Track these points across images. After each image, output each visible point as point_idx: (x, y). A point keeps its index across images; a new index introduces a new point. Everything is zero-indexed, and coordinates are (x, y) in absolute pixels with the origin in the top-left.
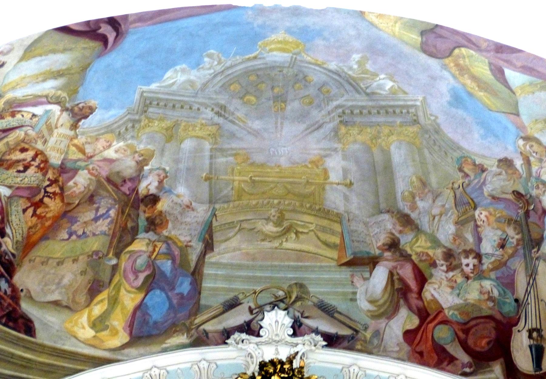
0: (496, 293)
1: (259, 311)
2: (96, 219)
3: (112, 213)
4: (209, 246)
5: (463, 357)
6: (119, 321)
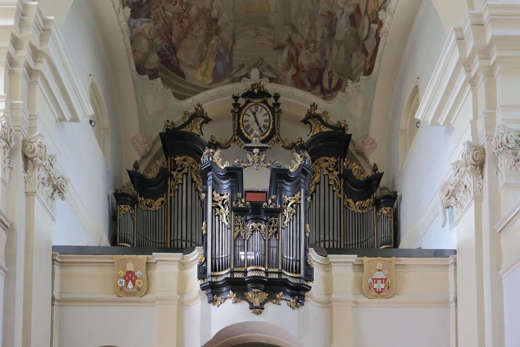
0: (319, 58)
1: (249, 69)
2: (200, 29)
3: (204, 26)
4: (234, 42)
5: (309, 84)
6: (209, 73)
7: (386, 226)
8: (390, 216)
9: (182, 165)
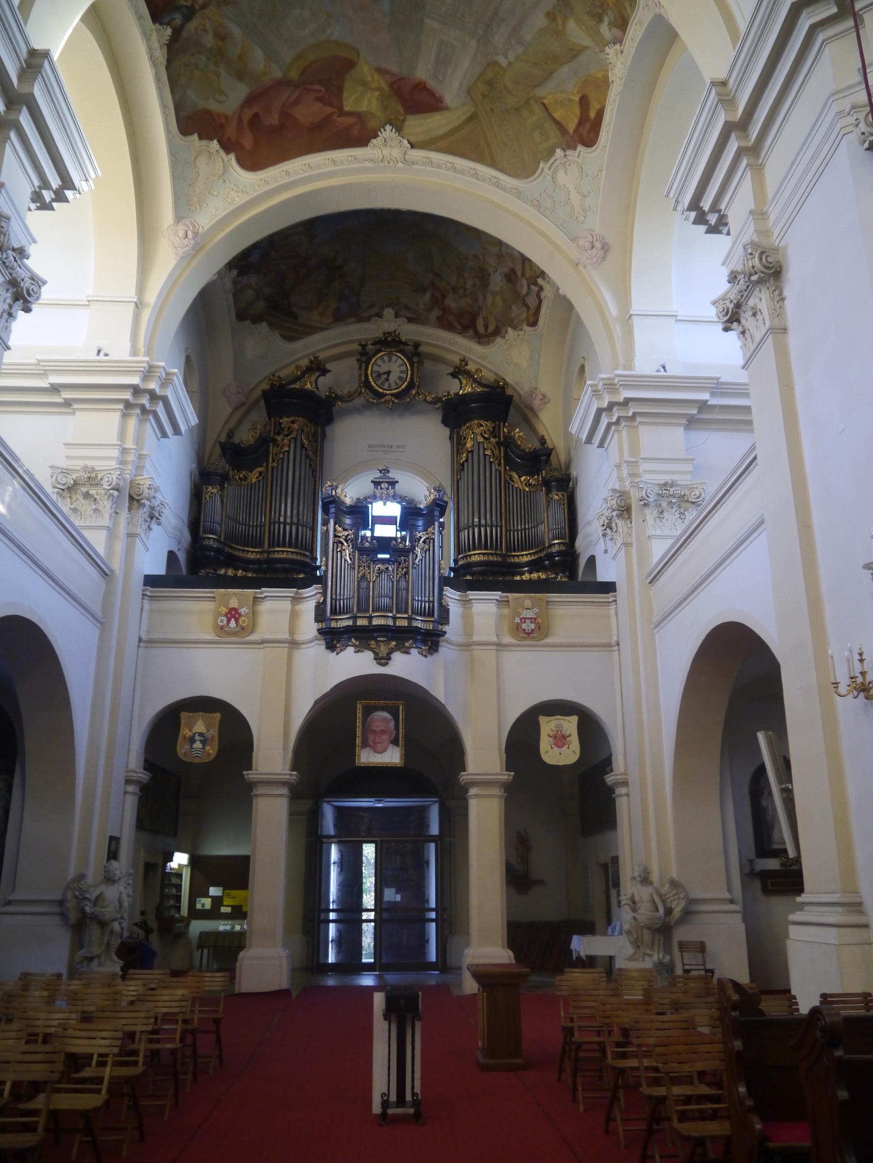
5: (458, 327)
7: (559, 515)
8: (562, 502)
9: (289, 428)
